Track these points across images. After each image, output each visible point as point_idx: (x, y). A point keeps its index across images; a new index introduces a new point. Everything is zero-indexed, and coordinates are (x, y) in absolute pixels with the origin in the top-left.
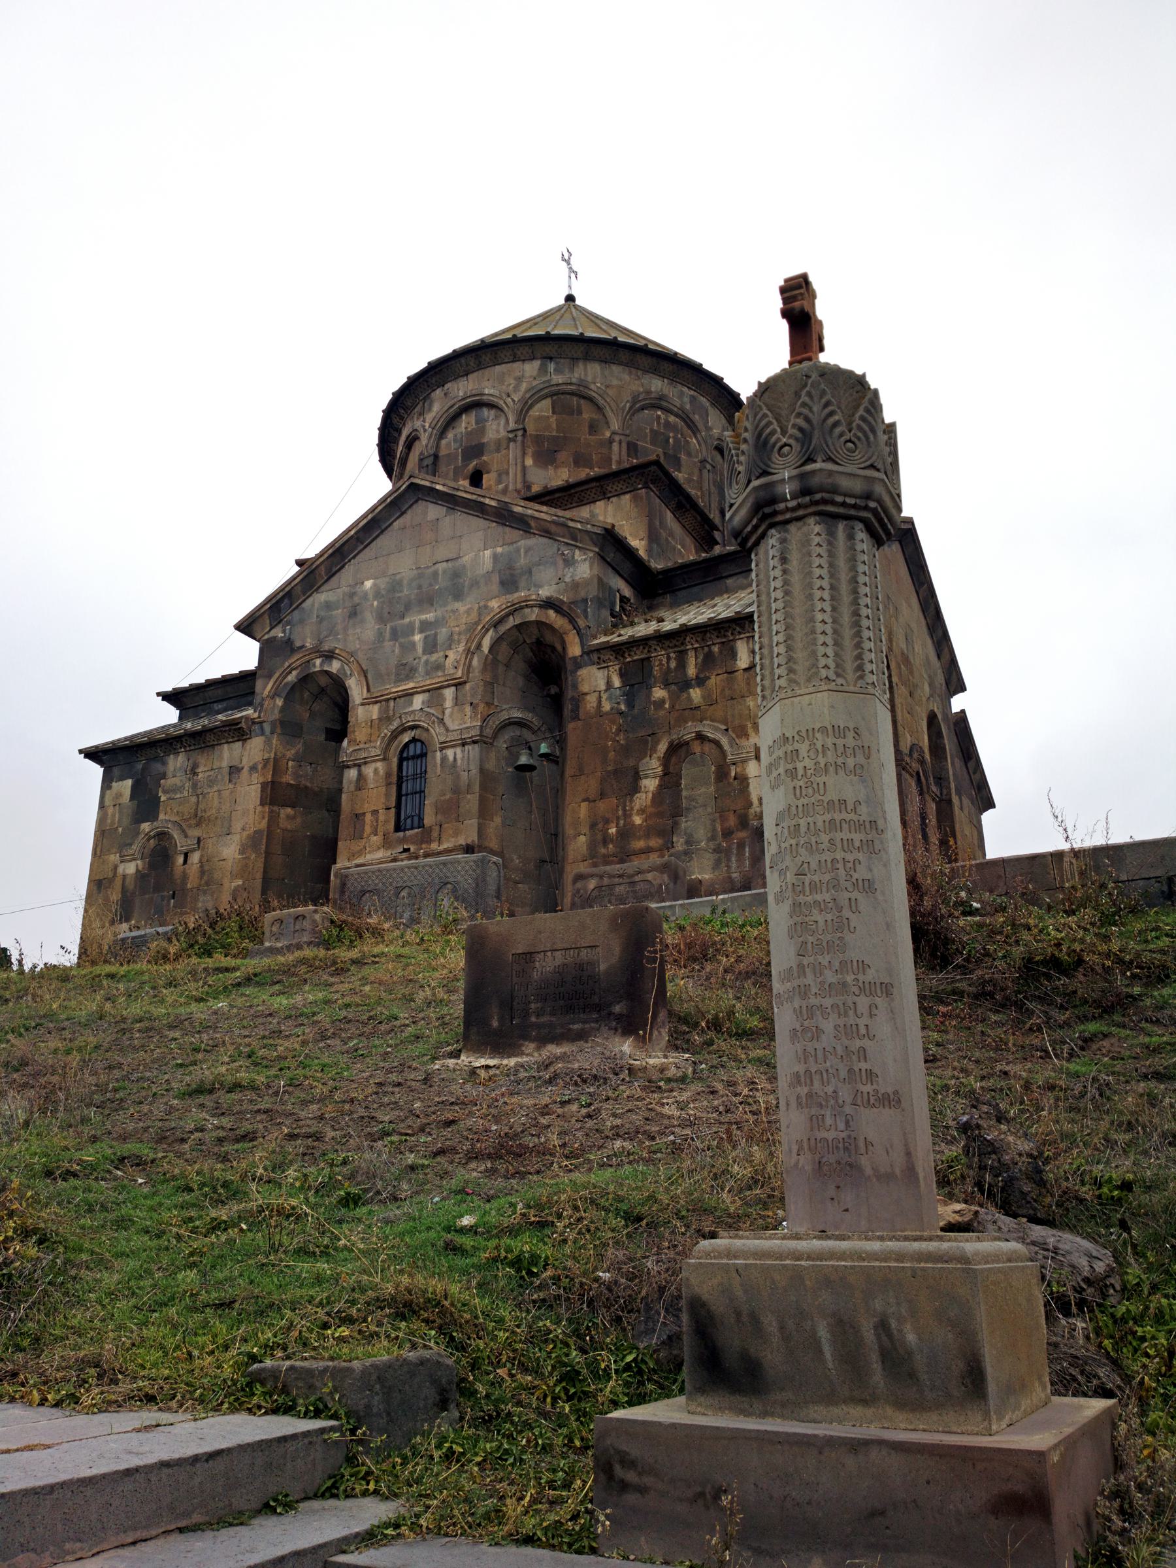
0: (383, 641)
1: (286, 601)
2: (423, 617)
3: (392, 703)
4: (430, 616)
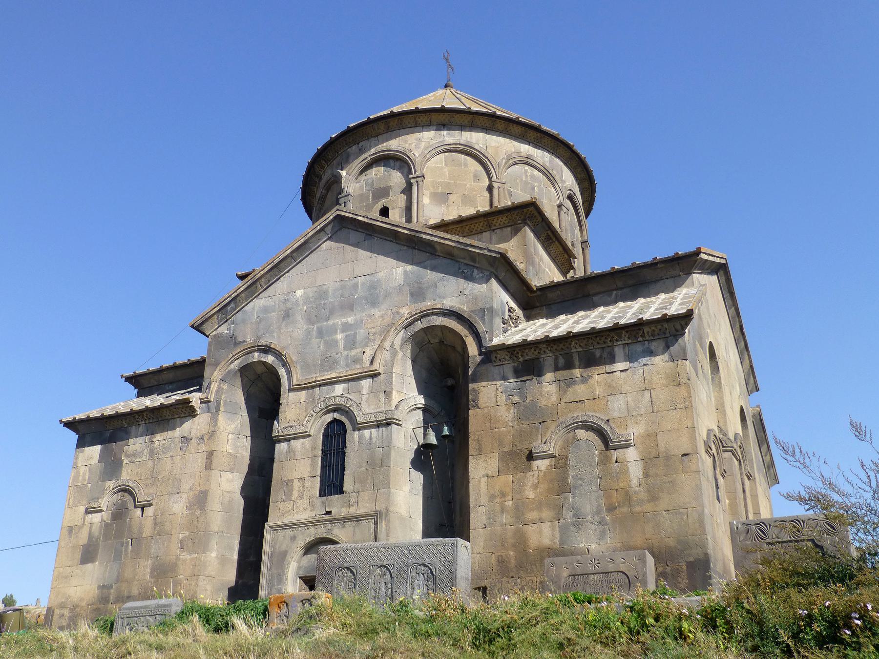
0: (311, 339)
1: (232, 305)
2: (344, 320)
4: (351, 319)
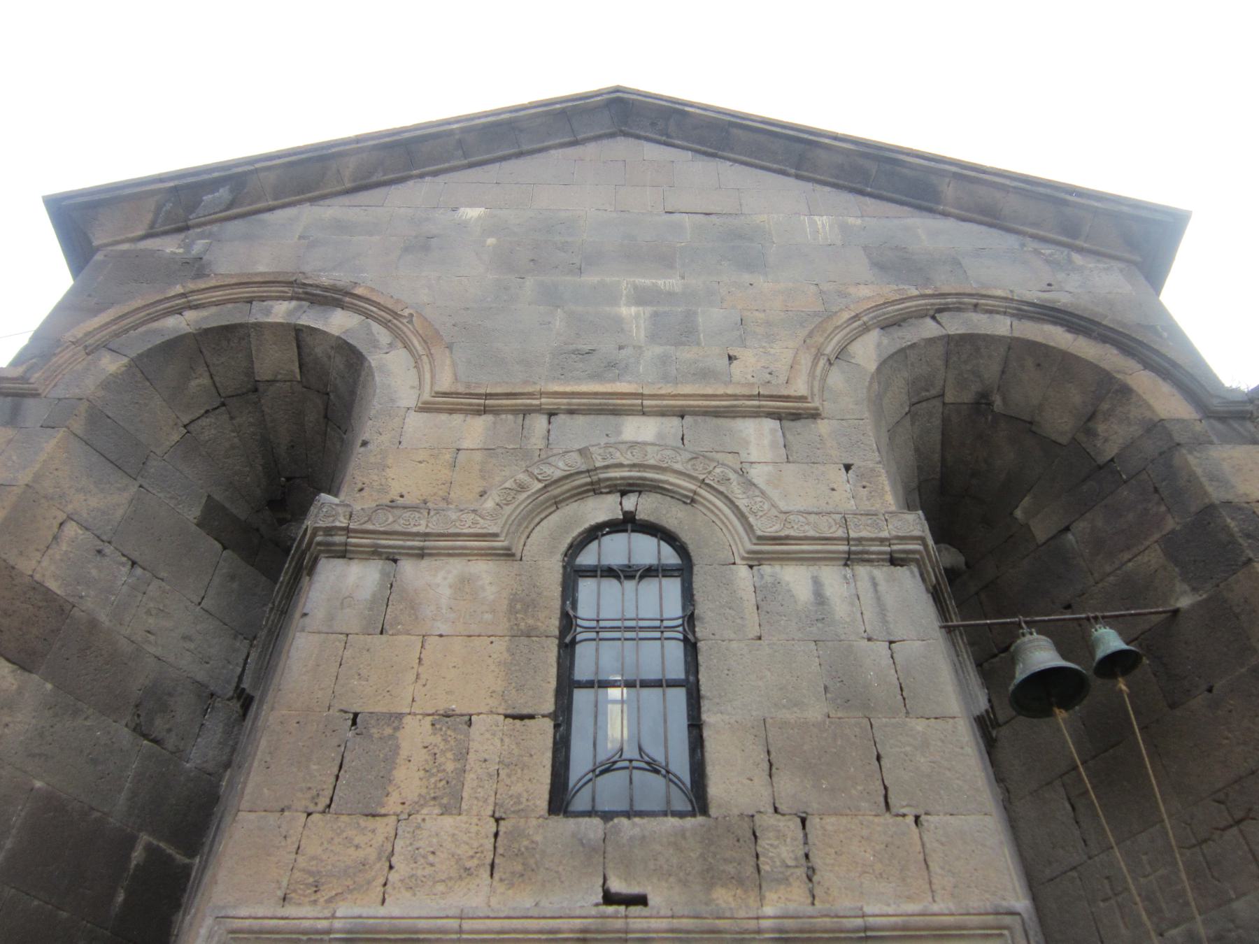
3: (540, 422)
4: (670, 283)
